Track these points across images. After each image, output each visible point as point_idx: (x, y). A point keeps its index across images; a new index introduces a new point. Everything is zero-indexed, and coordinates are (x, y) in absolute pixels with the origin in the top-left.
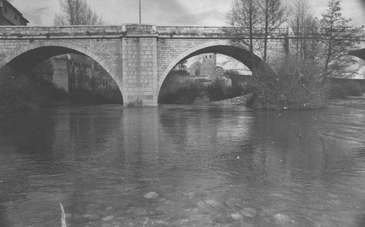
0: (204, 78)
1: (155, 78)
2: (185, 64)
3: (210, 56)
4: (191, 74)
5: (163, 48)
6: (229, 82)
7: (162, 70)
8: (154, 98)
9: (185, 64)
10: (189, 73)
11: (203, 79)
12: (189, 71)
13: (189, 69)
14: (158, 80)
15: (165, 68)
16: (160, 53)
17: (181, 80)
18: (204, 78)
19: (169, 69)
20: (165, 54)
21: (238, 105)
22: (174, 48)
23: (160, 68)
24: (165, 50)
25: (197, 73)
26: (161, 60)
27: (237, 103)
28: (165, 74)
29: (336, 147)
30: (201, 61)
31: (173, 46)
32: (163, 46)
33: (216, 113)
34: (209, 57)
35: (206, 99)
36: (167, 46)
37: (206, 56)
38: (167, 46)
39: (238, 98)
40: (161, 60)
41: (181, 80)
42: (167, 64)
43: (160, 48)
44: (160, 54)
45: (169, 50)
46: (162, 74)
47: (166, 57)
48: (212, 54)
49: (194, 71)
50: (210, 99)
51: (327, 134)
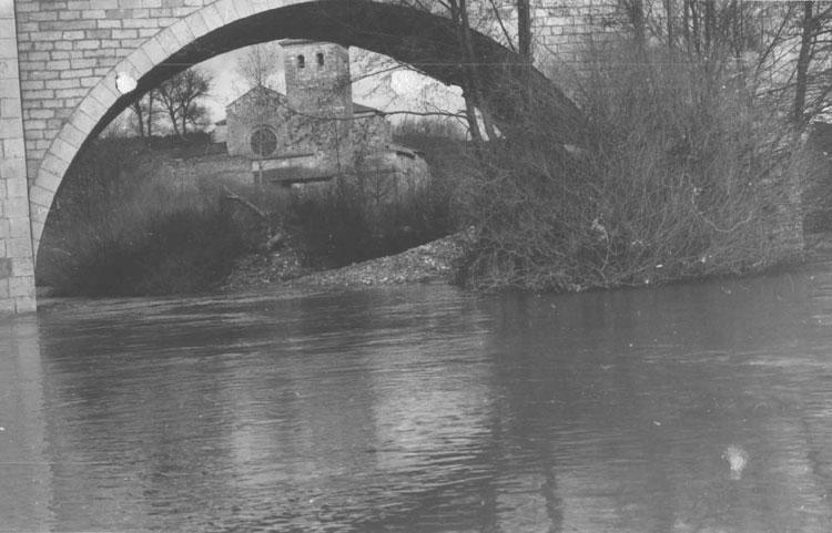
0: (296, 162)
1: (13, 172)
2: (199, 102)
3: (320, 56)
4: (231, 150)
5: (45, 27)
6: (410, 170)
7: (51, 135)
8: (16, 271)
9: (199, 102)
10: (223, 146)
11: (291, 170)
12: (221, 135)
13: (223, 123)
14: (31, 181)
15: (65, 121)
16: (33, 49)
17: (181, 178)
18: (296, 162)
19: (85, 124)
20: (56, 55)
21: (425, 281)
22: (102, 24)
23: (41, 125)
24: (56, 36)
25: (264, 143)
26: (39, 85)
27: (417, 274)
28: (67, 151)
29: (154, 450)
30: (277, 81)
31: (100, 14)
32: (43, 17)
33: (344, 324)
34: (311, 60)
35: (286, 263)
36: (63, 16)
37: (301, 58)
38: (63, 16)
39: (427, 247)
40: (39, 85)
41: (181, 178)
42: (71, 103)
43: (35, 27)
44: (34, 57)
45: (80, 35)
46: (48, 151)
47: (64, 65)
48: (326, 48)
49: (246, 136)
50: (304, 264)
51: (218, 367)
